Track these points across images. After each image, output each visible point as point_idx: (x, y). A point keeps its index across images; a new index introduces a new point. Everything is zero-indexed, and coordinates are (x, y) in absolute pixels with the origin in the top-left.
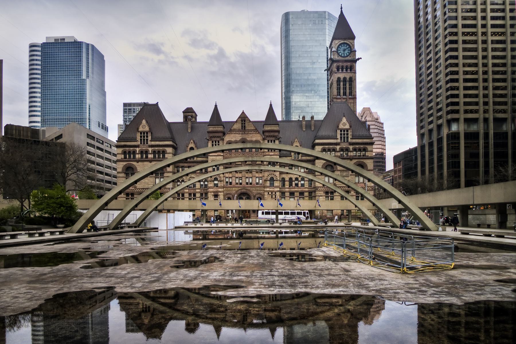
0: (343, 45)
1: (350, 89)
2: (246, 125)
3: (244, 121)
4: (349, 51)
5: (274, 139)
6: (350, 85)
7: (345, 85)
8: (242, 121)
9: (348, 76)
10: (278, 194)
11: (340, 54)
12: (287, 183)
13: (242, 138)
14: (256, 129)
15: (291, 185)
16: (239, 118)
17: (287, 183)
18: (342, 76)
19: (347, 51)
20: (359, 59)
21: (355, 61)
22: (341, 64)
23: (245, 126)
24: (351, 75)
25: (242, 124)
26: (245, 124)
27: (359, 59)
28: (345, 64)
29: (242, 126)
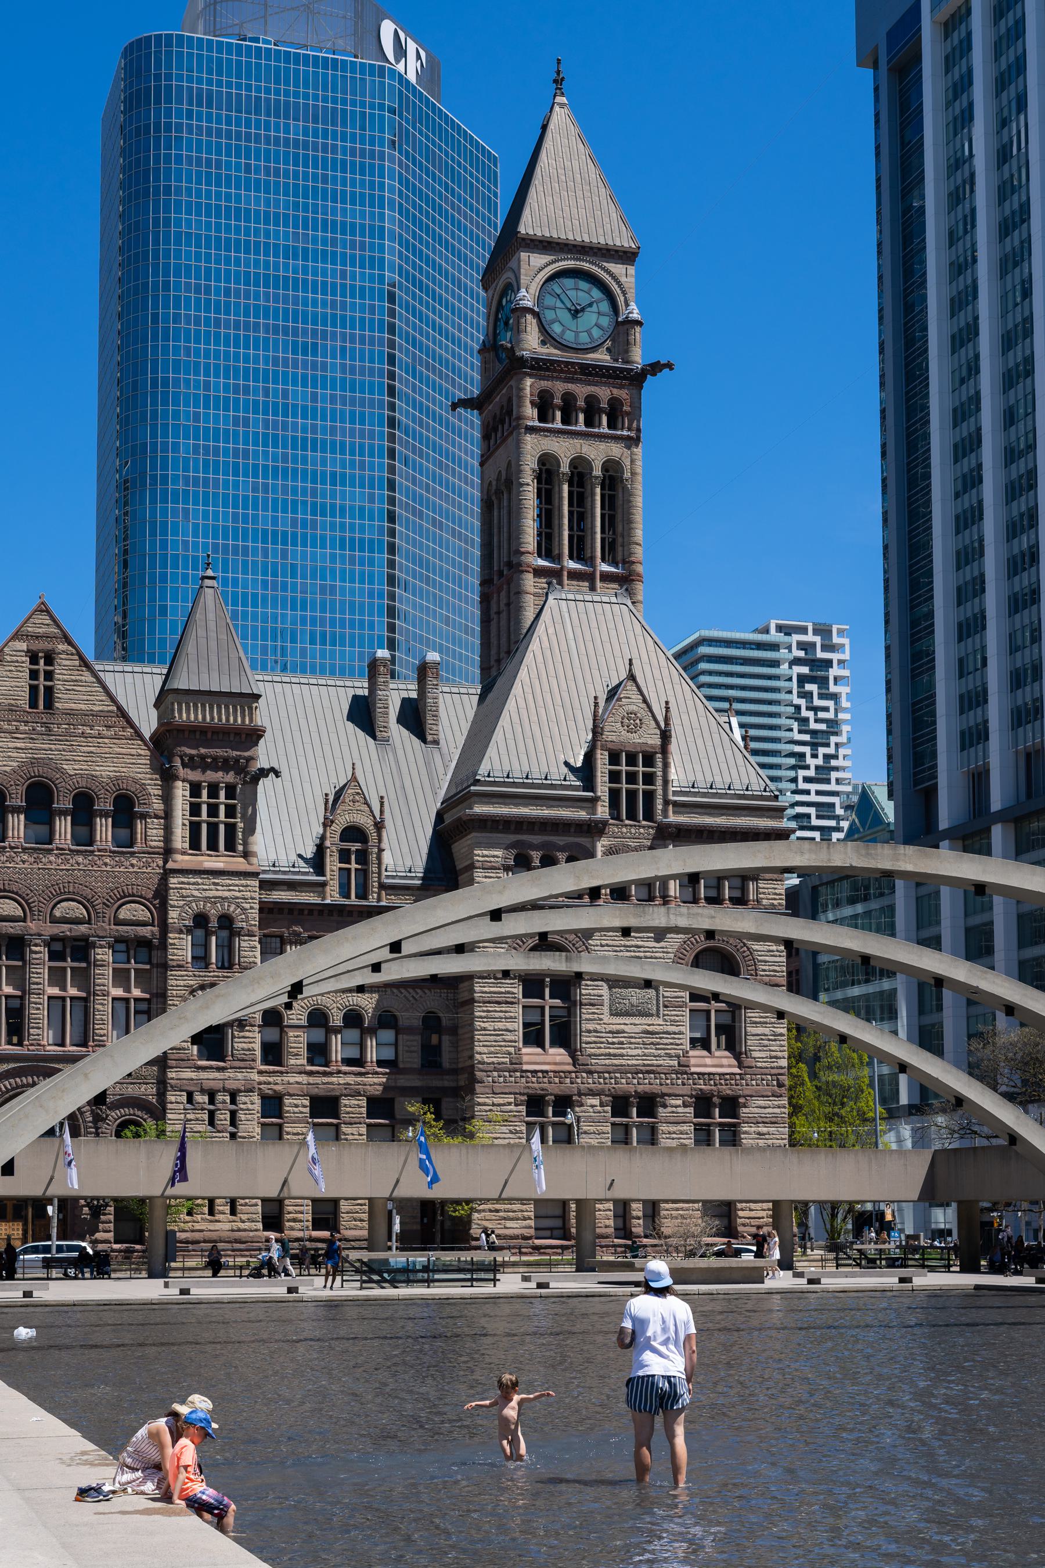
0: (569, 282)
1: (610, 522)
2: (58, 685)
3: (49, 660)
4: (605, 321)
5: (230, 777)
6: (609, 502)
7: (579, 500)
8: (34, 659)
9: (597, 453)
10: (252, 1104)
11: (557, 328)
12: (297, 1042)
13: (33, 762)
14: (122, 713)
15: (318, 1052)
16: (16, 636)
17: (297, 1042)
18: (564, 450)
19: (589, 318)
20: (655, 368)
21: (636, 379)
22: (559, 388)
23: (49, 691)
24: (616, 450)
25: (34, 675)
26: (49, 676)
27: (655, 368)
28: (581, 391)
29: (34, 690)
